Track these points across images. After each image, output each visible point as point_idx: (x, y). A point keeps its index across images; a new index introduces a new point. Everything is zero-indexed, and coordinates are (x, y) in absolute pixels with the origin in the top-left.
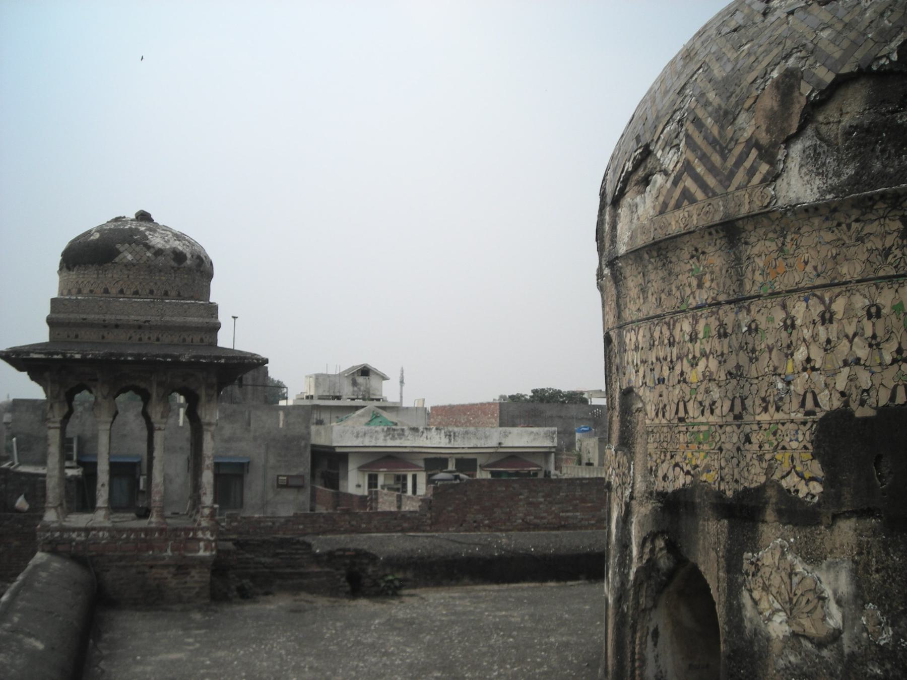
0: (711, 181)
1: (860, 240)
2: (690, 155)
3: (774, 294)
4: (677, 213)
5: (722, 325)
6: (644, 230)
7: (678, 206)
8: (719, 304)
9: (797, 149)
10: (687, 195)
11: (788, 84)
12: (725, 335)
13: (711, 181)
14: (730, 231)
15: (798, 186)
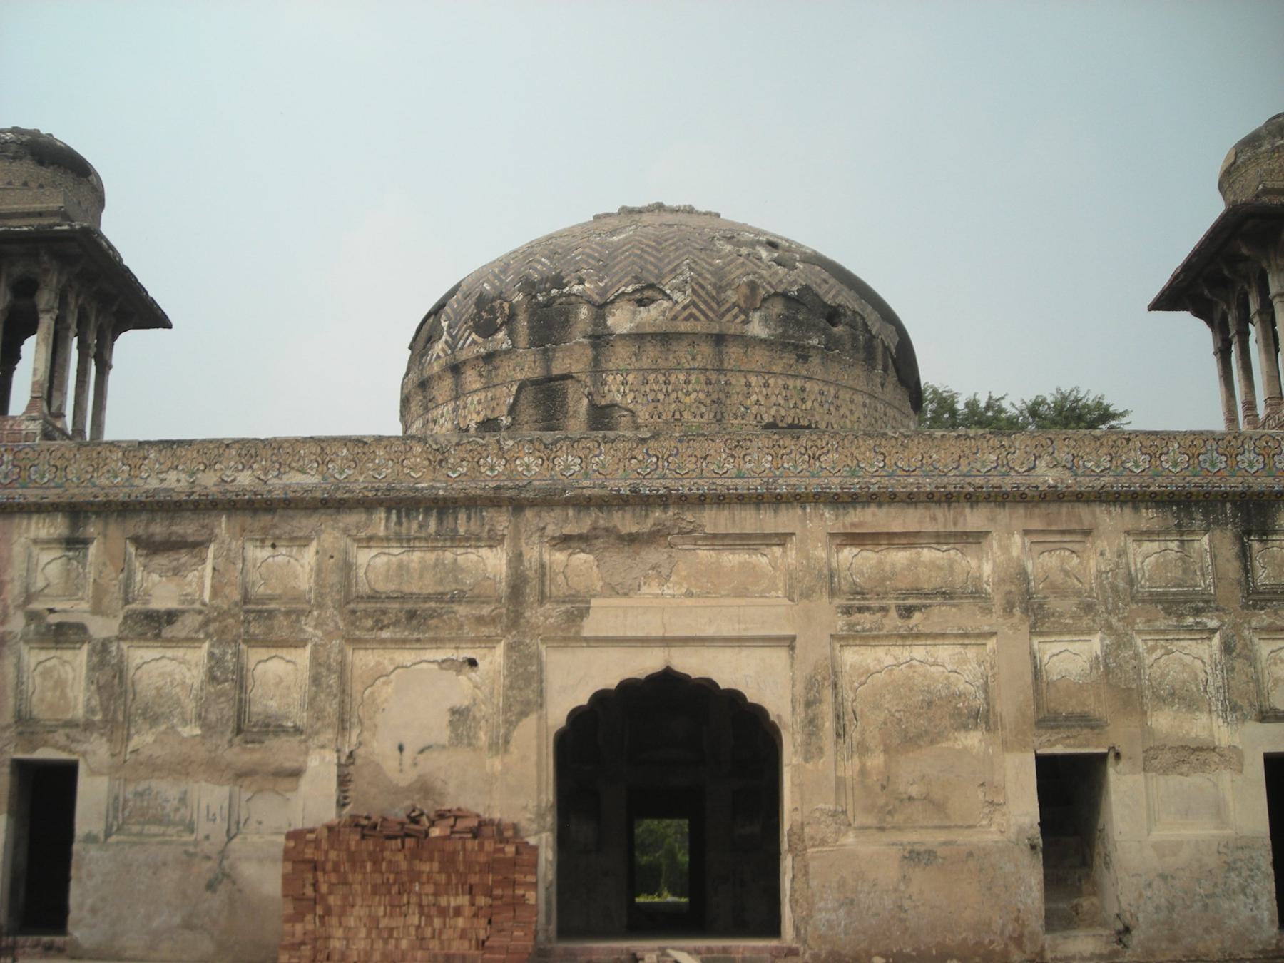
0: (711, 314)
1: (781, 358)
2: (696, 300)
3: (740, 371)
7: (686, 319)
9: (757, 314)
10: (691, 315)
11: (753, 286)
13: (711, 314)
14: (719, 340)
15: (757, 328)
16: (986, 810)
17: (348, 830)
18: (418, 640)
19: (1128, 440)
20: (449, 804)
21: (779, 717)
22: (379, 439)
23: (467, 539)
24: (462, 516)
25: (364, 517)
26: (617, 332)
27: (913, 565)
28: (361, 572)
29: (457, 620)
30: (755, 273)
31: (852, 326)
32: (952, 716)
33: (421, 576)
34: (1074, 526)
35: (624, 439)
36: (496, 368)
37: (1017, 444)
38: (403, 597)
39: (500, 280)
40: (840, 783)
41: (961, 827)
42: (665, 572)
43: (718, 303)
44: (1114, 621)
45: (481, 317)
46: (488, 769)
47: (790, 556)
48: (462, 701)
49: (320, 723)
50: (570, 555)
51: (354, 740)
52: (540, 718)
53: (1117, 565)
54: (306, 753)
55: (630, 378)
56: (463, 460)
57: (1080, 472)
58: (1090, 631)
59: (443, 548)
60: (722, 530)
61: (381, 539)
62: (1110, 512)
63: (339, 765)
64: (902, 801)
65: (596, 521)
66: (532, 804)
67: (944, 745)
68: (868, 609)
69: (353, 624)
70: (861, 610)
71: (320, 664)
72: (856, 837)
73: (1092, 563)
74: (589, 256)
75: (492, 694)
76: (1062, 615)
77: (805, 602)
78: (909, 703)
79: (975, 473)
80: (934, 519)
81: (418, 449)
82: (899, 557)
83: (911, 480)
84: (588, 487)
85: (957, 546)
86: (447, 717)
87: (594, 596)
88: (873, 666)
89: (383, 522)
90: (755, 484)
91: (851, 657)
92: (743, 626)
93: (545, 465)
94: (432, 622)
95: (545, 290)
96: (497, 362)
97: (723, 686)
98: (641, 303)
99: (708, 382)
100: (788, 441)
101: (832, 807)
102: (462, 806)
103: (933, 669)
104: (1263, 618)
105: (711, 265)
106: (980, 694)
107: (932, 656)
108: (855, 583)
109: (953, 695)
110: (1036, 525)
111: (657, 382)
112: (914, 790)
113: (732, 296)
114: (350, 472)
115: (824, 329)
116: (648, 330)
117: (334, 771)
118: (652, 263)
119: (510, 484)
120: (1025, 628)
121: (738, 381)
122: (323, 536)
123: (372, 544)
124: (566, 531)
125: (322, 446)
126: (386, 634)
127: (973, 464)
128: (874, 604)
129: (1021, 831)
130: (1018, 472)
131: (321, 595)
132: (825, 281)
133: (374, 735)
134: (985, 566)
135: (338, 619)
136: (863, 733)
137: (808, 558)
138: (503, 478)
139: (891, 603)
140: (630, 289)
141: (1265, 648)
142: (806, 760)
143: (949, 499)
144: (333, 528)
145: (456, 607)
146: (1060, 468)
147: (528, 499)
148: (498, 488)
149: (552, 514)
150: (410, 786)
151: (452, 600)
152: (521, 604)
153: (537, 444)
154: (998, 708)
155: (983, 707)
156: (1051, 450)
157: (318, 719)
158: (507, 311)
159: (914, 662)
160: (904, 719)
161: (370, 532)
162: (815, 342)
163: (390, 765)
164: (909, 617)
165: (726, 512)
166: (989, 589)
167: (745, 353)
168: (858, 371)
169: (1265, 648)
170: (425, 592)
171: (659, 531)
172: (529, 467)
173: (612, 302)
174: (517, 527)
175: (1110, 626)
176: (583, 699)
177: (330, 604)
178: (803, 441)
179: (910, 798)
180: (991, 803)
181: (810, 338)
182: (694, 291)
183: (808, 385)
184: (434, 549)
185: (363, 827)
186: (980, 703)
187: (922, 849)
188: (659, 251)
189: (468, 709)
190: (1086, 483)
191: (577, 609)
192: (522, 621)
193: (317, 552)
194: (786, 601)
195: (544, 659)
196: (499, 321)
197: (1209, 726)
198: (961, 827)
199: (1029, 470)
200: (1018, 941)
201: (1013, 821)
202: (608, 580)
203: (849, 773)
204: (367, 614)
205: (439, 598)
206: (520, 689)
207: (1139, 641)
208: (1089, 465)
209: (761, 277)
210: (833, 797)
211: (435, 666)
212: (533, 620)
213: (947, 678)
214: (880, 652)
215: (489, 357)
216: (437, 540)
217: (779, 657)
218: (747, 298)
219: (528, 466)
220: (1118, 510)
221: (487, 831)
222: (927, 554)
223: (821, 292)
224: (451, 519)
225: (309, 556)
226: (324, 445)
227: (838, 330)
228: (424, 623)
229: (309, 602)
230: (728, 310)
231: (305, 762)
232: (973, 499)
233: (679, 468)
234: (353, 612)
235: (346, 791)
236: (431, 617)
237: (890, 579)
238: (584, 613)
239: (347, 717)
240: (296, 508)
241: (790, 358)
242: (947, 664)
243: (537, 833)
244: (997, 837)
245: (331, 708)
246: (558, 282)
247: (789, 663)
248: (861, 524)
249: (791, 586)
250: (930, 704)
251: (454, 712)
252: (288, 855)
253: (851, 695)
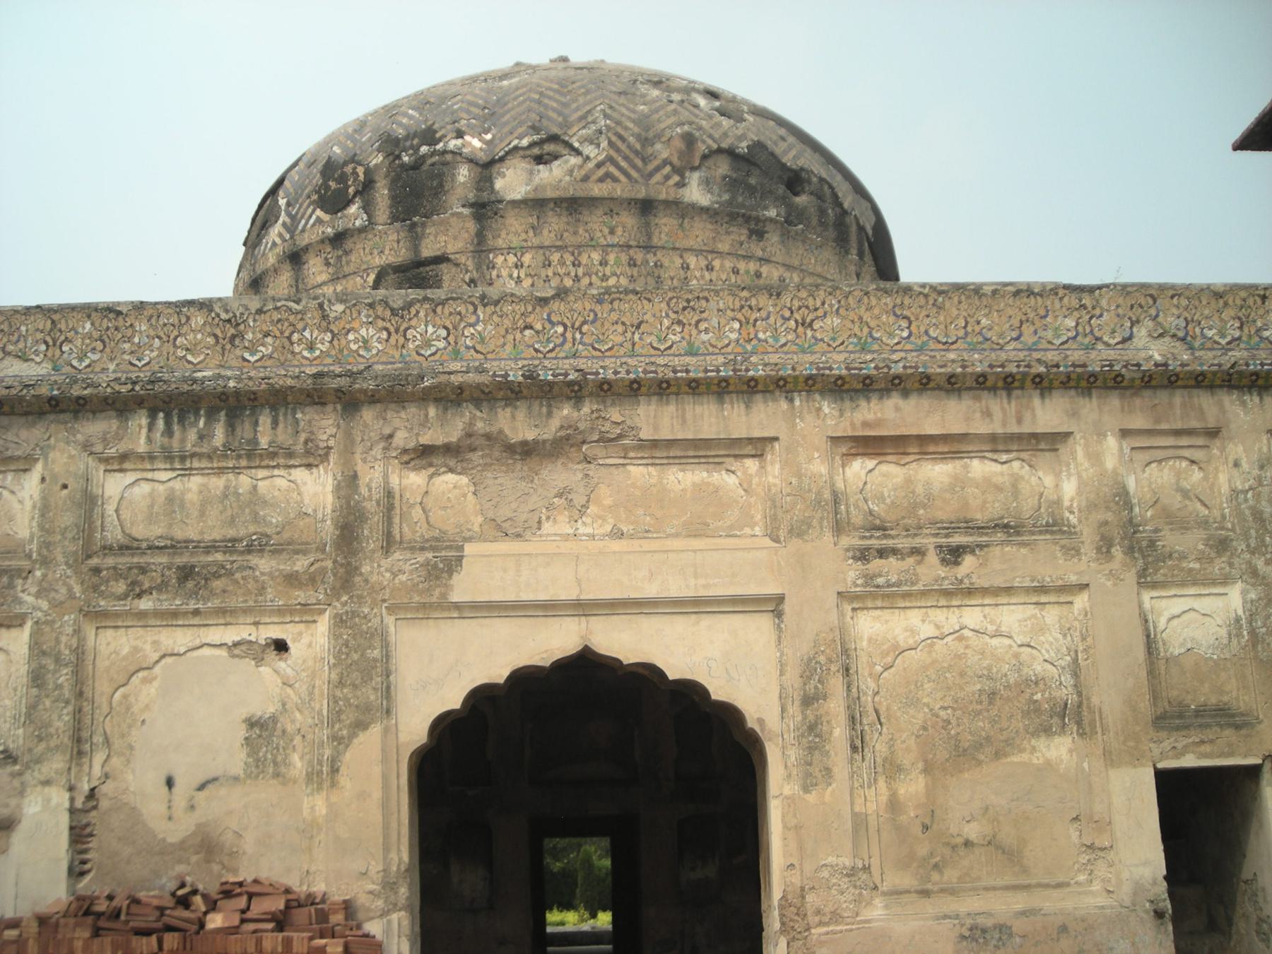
0: (634, 174)
1: (728, 233)
3: (674, 249)
4: (600, 185)
5: (631, 259)
6: (556, 187)
7: (601, 180)
8: (630, 247)
10: (608, 175)
11: (689, 140)
12: (635, 265)
13: (634, 174)
14: (646, 207)
15: (695, 193)
16: (1084, 859)
17: (72, 921)
18: (196, 613)
19: (1264, 298)
21: (761, 721)
22: (140, 306)
23: (273, 455)
24: (265, 420)
25: (115, 424)
26: (508, 198)
27: (958, 483)
28: (110, 509)
29: (256, 580)
30: (691, 123)
31: (820, 197)
32: (1026, 714)
33: (202, 513)
34: (1194, 424)
35: (513, 298)
36: (347, 253)
37: (1104, 303)
38: (174, 546)
39: (355, 141)
40: (859, 822)
41: (1047, 886)
42: (579, 500)
43: (645, 160)
44: (1260, 563)
45: (327, 188)
46: (306, 812)
47: (772, 473)
48: (263, 707)
49: (43, 745)
50: (431, 477)
51: (97, 770)
52: (386, 731)
53: (1259, 480)
54: (21, 793)
55: (527, 259)
56: (267, 335)
57: (1197, 344)
58: (1226, 580)
59: (236, 470)
60: (665, 434)
61: (141, 458)
62: (1244, 403)
63: (72, 811)
64: (954, 847)
65: (471, 424)
66: (376, 867)
67: (1015, 759)
68: (895, 551)
69: (95, 588)
70: (882, 553)
71: (44, 653)
72: (886, 907)
73: (1223, 478)
74: (471, 103)
75: (311, 693)
76: (1183, 557)
77: (795, 543)
78: (961, 695)
79: (1044, 345)
80: (988, 414)
81: (198, 319)
82: (936, 473)
83: (952, 356)
84: (459, 371)
85: (1024, 455)
86: (242, 732)
87: (469, 539)
88: (903, 639)
89: (144, 431)
90: (717, 364)
91: (871, 627)
92: (702, 581)
93: (392, 341)
94: (217, 584)
95: (412, 147)
96: (349, 244)
97: (672, 675)
98: (539, 160)
99: (632, 263)
100: (763, 300)
101: (847, 861)
102: (263, 875)
103: (995, 642)
105: (634, 111)
106: (1068, 680)
107: (992, 622)
108: (871, 512)
109: (1027, 681)
110: (1139, 422)
111: (563, 264)
112: (973, 831)
113: (662, 151)
114: (95, 357)
115: (784, 198)
116: (550, 194)
117: (64, 821)
118: (554, 110)
119: (338, 370)
120: (1131, 577)
121: (672, 263)
122: (51, 455)
123: (127, 465)
124: (425, 439)
125: (54, 318)
126: (145, 604)
127: (1040, 333)
128: (903, 543)
129: (1138, 889)
130: (1107, 344)
131: (47, 545)
132: (783, 139)
133: (128, 761)
134: (1065, 484)
135: (72, 582)
136: (891, 743)
137: (799, 476)
138: (329, 360)
139: (928, 541)
140: (525, 142)
142: (806, 789)
143: (1008, 383)
144: (68, 443)
145: (254, 560)
146: (1167, 339)
147: (365, 392)
148: (319, 375)
149: (403, 415)
150: (183, 842)
151: (249, 550)
152: (354, 553)
153: (380, 310)
154: (1095, 700)
155: (1073, 699)
156: (1153, 312)
157: (40, 739)
158: (362, 177)
159: (966, 632)
160: (954, 722)
161: (123, 447)
162: (772, 213)
163: (153, 808)
164: (957, 563)
165: (672, 408)
166: (1073, 519)
167: (681, 225)
168: (828, 254)
170: (207, 537)
171: (568, 438)
172: (369, 345)
173: (502, 159)
174: (348, 435)
175: (1254, 573)
176: (454, 700)
177: (60, 558)
178: (786, 299)
179: (968, 843)
180: (1091, 847)
181: (766, 208)
182: (611, 144)
183: (765, 270)
184: (221, 471)
185: (99, 915)
186: (1066, 693)
187: (989, 923)
188: (564, 95)
189: (274, 719)
190: (1208, 360)
191: (444, 559)
192: (357, 579)
193: (43, 479)
194: (768, 542)
195: (392, 639)
196: (351, 190)
198: (1047, 886)
199: (1124, 341)
201: (1125, 875)
202: (490, 515)
203: (871, 807)
204: (117, 573)
205: (229, 545)
206: (355, 686)
208: (1210, 333)
209: (700, 128)
210: (848, 845)
211: (223, 653)
212: (374, 578)
213: (1016, 656)
214: (914, 617)
215: (338, 239)
216: (226, 456)
217: (758, 628)
218: (681, 155)
219: (365, 342)
220: (1256, 399)
221: (300, 916)
222: (979, 468)
223: (778, 151)
224: (247, 426)
225: (30, 486)
226: (56, 317)
227: (802, 200)
228: (206, 586)
229: (29, 556)
230: (658, 169)
231: (19, 806)
232: (1043, 384)
233: (599, 341)
234: (96, 571)
235: (85, 851)
236: (217, 576)
237: (924, 506)
238: (453, 565)
239: (85, 734)
240: (12, 413)
241: (741, 233)
242: (1016, 634)
243: (384, 913)
244: (1102, 900)
245: (61, 721)
246: (429, 136)
247: (774, 637)
248: (878, 423)
249: (774, 518)
250: (993, 695)
251: (252, 723)
253: (872, 685)
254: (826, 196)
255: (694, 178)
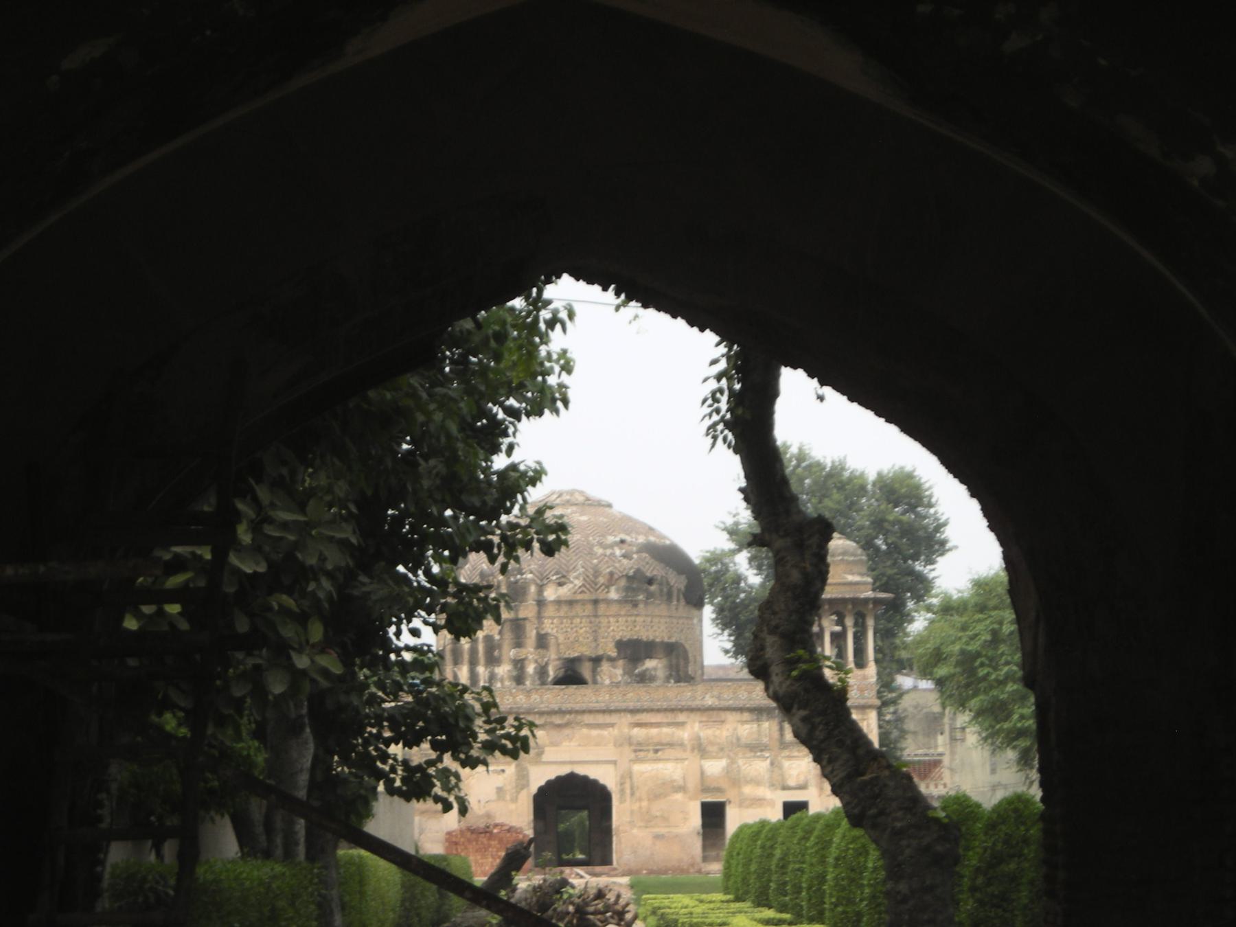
11: (611, 574)
14: (596, 602)
15: (613, 595)
20: (498, 821)
31: (661, 584)
40: (632, 812)
47: (615, 732)
48: (500, 784)
82: (654, 731)
84: (543, 707)
90: (602, 706)
91: (637, 768)
98: (560, 584)
104: (786, 753)
113: (601, 580)
121: (604, 621)
141: (786, 764)
143: (672, 710)
168: (663, 607)
169: (786, 764)
176: (542, 783)
186: (681, 783)
190: (724, 704)
197: (764, 792)
200: (692, 865)
207: (740, 762)
217: (611, 768)
222: (665, 730)
227: (653, 588)
232: (682, 710)
241: (628, 607)
242: (670, 769)
250: (664, 784)
252: (447, 840)
254: (664, 583)
255: (613, 589)
